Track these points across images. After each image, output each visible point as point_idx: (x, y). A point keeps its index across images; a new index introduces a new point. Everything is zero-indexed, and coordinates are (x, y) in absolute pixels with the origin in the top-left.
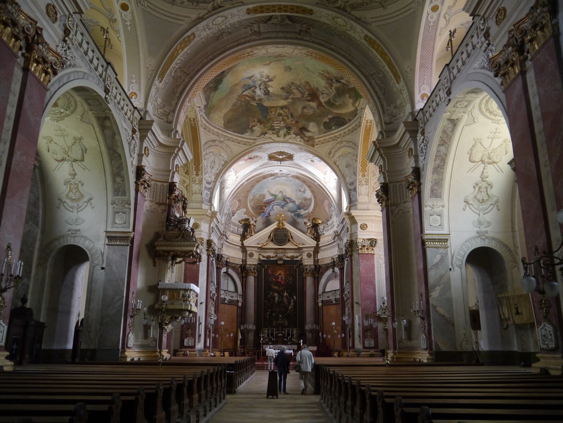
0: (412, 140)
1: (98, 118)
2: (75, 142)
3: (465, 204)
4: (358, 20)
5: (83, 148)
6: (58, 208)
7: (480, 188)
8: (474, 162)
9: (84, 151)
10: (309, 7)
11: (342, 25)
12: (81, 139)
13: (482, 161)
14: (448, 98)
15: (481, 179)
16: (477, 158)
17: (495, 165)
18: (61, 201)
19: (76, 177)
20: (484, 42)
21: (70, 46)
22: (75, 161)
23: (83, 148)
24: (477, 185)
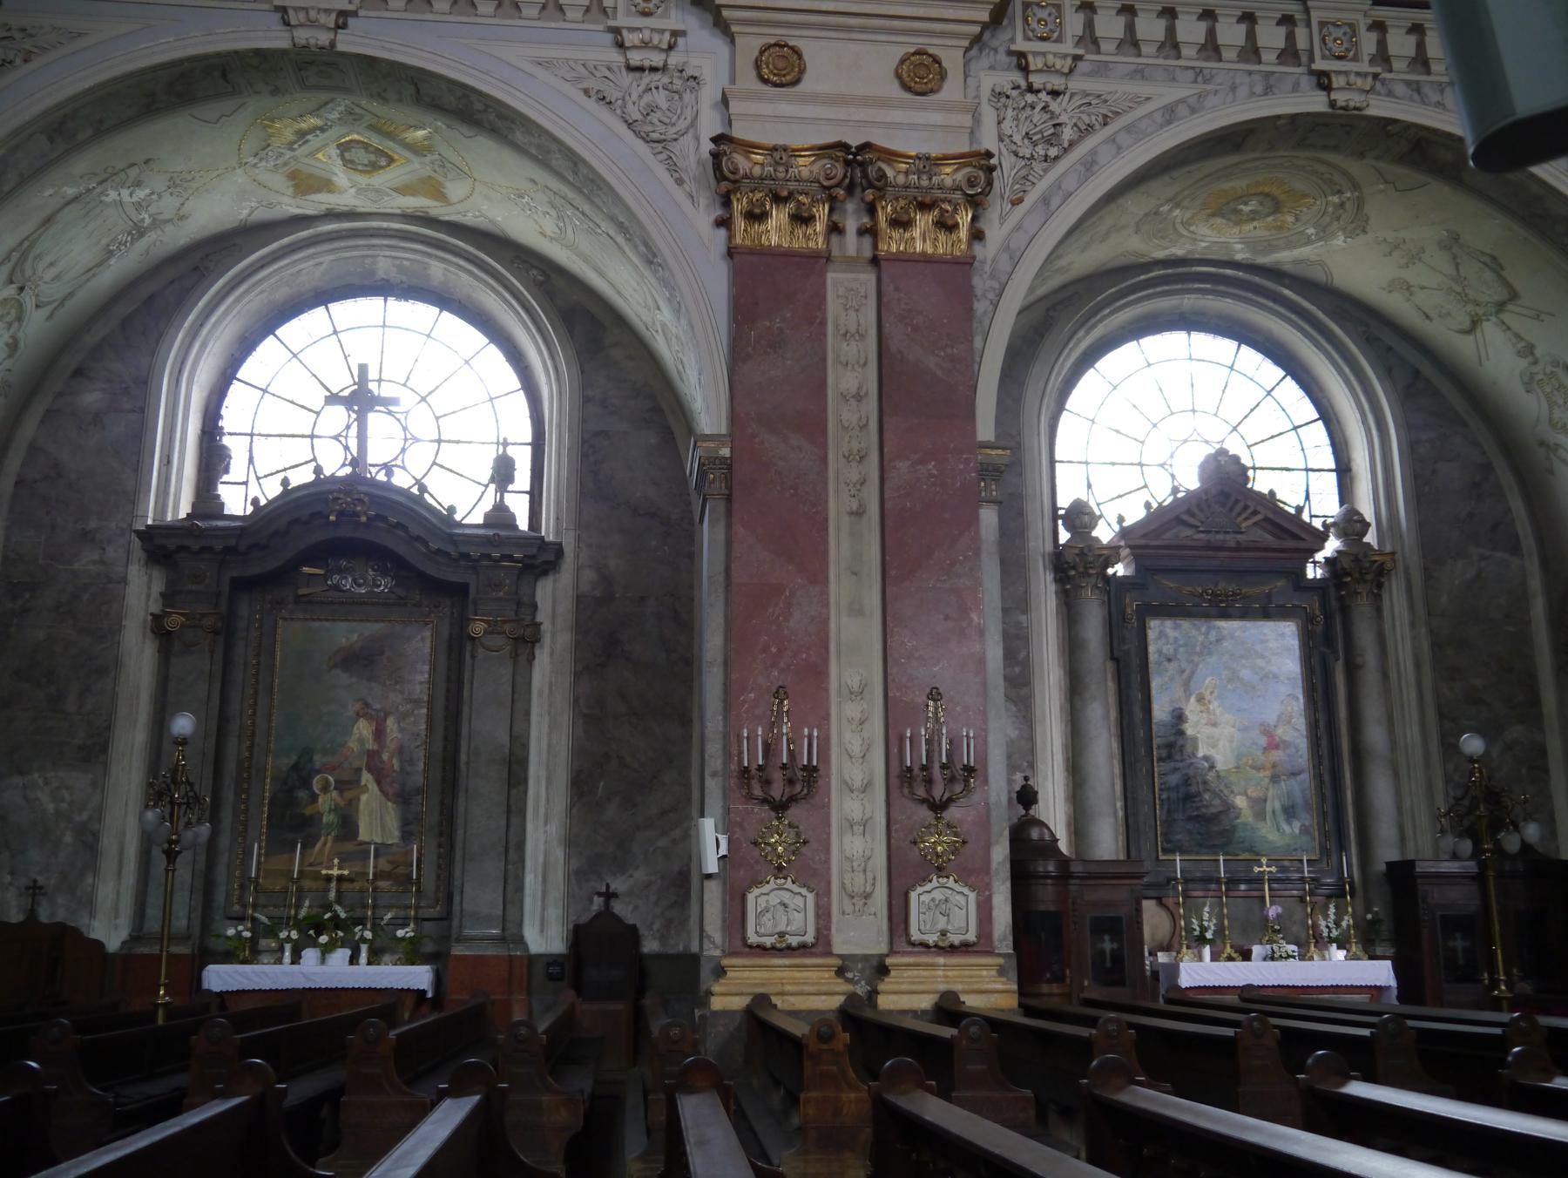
1: (1407, 159)
2: (1455, 258)
5: (1486, 259)
6: (1551, 471)
9: (1495, 265)
12: (1455, 238)
18: (1548, 446)
19: (1538, 352)
21: (1056, 82)
22: (1500, 307)
23: (1486, 259)
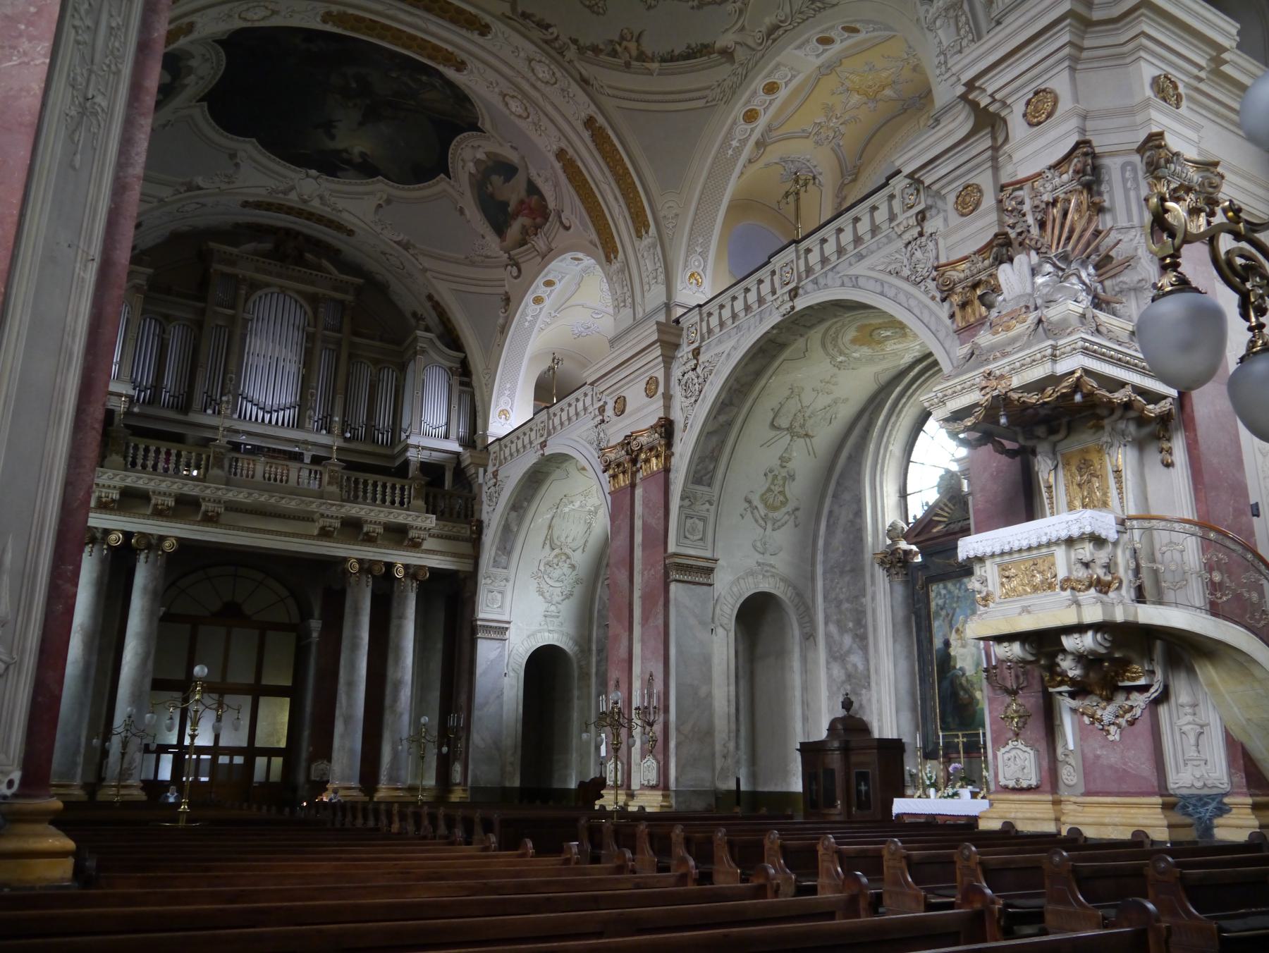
0: (664, 361)
3: (747, 505)
4: (584, 82)
7: (775, 477)
8: (778, 428)
10: (488, 19)
13: (790, 429)
14: (791, 304)
15: (779, 462)
16: (784, 422)
17: (808, 440)
24: (771, 471)
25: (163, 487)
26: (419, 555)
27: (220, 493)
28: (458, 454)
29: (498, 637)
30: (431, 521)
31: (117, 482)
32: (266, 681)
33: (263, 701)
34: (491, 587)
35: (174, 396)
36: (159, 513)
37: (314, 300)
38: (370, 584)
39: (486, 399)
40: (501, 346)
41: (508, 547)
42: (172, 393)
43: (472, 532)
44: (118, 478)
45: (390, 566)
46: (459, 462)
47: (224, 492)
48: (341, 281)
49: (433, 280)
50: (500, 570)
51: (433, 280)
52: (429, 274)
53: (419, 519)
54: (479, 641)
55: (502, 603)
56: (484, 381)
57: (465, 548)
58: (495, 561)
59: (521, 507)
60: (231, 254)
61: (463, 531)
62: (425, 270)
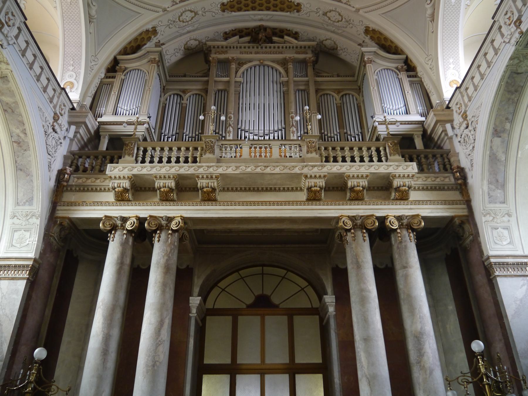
11: (337, 21)
20: (463, 122)
25: (163, 171)
26: (409, 207)
27: (211, 170)
28: (421, 123)
29: (519, 273)
30: (413, 167)
31: (126, 172)
32: (300, 359)
33: (300, 379)
34: (494, 224)
35: (192, 137)
36: (166, 198)
37: (284, 63)
38: (367, 238)
39: (434, 78)
40: (435, 32)
41: (501, 180)
42: (190, 135)
43: (456, 179)
44: (126, 170)
45: (382, 220)
46: (425, 131)
47: (215, 168)
48: (301, 47)
49: (366, 15)
50: (498, 205)
51: (366, 15)
52: (361, 12)
53: (400, 168)
54: (498, 279)
55: (511, 238)
56: (427, 67)
57: (455, 195)
58: (490, 197)
59: (504, 131)
60: (222, 47)
61: (447, 180)
62: (358, 10)
